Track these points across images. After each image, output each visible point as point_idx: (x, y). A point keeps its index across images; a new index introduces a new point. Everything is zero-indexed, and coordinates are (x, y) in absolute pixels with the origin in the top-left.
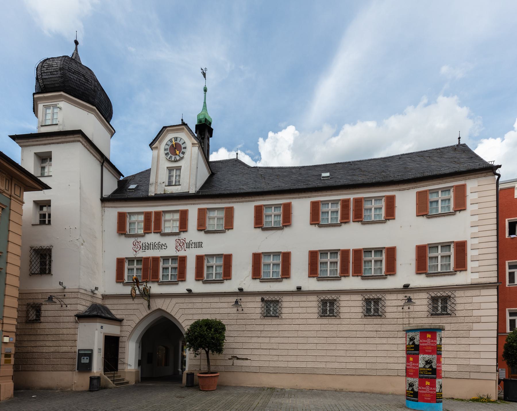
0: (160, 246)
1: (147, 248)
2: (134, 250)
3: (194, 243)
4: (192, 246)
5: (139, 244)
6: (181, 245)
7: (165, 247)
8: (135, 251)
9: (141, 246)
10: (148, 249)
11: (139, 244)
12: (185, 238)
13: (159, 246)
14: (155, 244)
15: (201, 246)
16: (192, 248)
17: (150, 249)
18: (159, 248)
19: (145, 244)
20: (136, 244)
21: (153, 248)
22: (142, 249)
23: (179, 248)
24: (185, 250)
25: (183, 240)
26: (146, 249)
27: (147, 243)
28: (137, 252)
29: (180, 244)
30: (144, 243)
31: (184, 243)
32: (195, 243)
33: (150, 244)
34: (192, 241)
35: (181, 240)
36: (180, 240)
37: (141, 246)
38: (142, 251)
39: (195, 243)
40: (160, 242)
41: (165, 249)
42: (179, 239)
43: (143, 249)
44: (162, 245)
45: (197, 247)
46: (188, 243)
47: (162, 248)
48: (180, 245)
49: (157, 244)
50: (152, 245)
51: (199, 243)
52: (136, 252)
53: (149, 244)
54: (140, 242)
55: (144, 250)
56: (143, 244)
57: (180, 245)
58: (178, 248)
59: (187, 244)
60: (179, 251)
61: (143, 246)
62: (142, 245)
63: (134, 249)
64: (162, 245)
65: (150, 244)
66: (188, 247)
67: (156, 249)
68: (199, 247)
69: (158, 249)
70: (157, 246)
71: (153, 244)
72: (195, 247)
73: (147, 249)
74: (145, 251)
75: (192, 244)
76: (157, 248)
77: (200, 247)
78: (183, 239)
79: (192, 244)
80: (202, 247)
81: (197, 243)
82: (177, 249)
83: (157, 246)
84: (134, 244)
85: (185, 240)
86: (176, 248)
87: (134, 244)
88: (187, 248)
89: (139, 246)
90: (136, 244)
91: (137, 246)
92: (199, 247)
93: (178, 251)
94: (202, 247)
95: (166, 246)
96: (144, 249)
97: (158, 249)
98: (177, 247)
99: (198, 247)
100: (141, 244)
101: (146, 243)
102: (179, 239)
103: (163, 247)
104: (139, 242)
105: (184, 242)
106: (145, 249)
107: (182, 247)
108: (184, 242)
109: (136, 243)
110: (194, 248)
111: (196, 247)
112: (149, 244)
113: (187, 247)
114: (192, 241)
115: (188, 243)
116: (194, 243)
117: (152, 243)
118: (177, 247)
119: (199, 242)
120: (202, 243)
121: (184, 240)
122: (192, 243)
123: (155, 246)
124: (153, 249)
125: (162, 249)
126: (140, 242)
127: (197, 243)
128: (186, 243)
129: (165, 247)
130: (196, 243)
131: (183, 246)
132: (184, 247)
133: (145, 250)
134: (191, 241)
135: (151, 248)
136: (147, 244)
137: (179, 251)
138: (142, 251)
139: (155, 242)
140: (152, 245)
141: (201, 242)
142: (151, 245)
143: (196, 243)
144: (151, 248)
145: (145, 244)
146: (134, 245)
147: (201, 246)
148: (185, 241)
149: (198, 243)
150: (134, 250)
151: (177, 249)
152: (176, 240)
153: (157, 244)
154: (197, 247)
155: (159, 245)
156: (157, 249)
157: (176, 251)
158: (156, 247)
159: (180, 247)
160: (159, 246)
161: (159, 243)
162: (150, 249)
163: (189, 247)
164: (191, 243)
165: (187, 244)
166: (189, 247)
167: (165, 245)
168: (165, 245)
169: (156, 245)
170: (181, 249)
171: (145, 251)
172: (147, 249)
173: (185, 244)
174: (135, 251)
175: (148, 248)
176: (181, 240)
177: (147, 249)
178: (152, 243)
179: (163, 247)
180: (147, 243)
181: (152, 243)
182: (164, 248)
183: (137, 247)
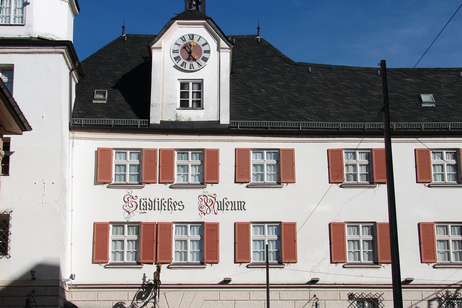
0: (172, 205)
1: (148, 207)
2: (125, 210)
3: (231, 202)
6: (209, 204)
7: (181, 208)
8: (128, 212)
9: (138, 204)
10: (150, 210)
12: (215, 194)
13: (171, 205)
14: (163, 201)
15: (242, 208)
16: (228, 210)
17: (155, 210)
20: (128, 201)
21: (160, 208)
22: (141, 209)
23: (205, 209)
24: (216, 214)
25: (211, 196)
26: (148, 208)
27: (149, 199)
29: (206, 204)
30: (144, 199)
31: (214, 201)
33: (155, 201)
34: (227, 199)
35: (209, 197)
36: (206, 196)
38: (140, 211)
40: (171, 199)
41: (181, 210)
42: (204, 196)
43: (142, 207)
44: (175, 204)
45: (236, 208)
46: (220, 202)
47: (175, 207)
48: (207, 205)
49: (166, 202)
50: (158, 202)
51: (239, 203)
52: (129, 213)
53: (153, 201)
54: (136, 196)
55: (143, 211)
56: (142, 200)
57: (207, 205)
58: (204, 209)
60: (205, 214)
61: (142, 203)
62: (140, 202)
64: (175, 204)
65: (155, 201)
66: (221, 209)
67: (165, 210)
68: (240, 208)
69: (169, 210)
71: (160, 201)
72: (233, 208)
75: (228, 204)
76: (166, 208)
77: (241, 210)
78: (213, 195)
79: (228, 204)
80: (245, 210)
81: (236, 203)
82: (201, 211)
84: (126, 200)
85: (214, 197)
87: (126, 200)
88: (219, 210)
90: (128, 201)
91: (130, 203)
92: (240, 208)
94: (245, 210)
95: (183, 205)
96: (144, 209)
97: (169, 210)
98: (201, 207)
100: (138, 201)
101: (146, 199)
102: (204, 196)
103: (177, 207)
104: (134, 197)
105: (213, 200)
106: (145, 208)
108: (213, 200)
110: (232, 210)
111: (235, 210)
112: (153, 201)
113: (219, 208)
114: (227, 199)
115: (220, 202)
116: (231, 202)
117: (158, 199)
118: (201, 207)
119: (240, 201)
120: (245, 203)
121: (213, 197)
122: (228, 202)
123: (163, 206)
124: (159, 209)
125: (175, 210)
127: (236, 203)
130: (234, 202)
132: (214, 208)
133: (145, 211)
134: (225, 199)
135: (156, 208)
136: (148, 201)
140: (158, 202)
141: (243, 202)
142: (156, 203)
143: (234, 202)
144: (156, 208)
145: (145, 200)
146: (126, 202)
147: (242, 208)
148: (215, 198)
149: (238, 202)
150: (125, 210)
151: (201, 211)
152: (200, 196)
153: (166, 202)
154: (236, 208)
155: (170, 204)
156: (167, 210)
157: (201, 214)
158: (165, 206)
159: (207, 207)
160: (171, 205)
161: (170, 200)
162: (155, 210)
163: (222, 208)
164: (225, 202)
166: (222, 208)
167: (180, 204)
168: (180, 203)
169: (165, 204)
172: (149, 209)
173: (216, 204)
174: (128, 212)
175: (150, 208)
176: (209, 197)
178: (156, 200)
179: (177, 207)
180: (149, 199)
181: (158, 199)
182: (179, 209)
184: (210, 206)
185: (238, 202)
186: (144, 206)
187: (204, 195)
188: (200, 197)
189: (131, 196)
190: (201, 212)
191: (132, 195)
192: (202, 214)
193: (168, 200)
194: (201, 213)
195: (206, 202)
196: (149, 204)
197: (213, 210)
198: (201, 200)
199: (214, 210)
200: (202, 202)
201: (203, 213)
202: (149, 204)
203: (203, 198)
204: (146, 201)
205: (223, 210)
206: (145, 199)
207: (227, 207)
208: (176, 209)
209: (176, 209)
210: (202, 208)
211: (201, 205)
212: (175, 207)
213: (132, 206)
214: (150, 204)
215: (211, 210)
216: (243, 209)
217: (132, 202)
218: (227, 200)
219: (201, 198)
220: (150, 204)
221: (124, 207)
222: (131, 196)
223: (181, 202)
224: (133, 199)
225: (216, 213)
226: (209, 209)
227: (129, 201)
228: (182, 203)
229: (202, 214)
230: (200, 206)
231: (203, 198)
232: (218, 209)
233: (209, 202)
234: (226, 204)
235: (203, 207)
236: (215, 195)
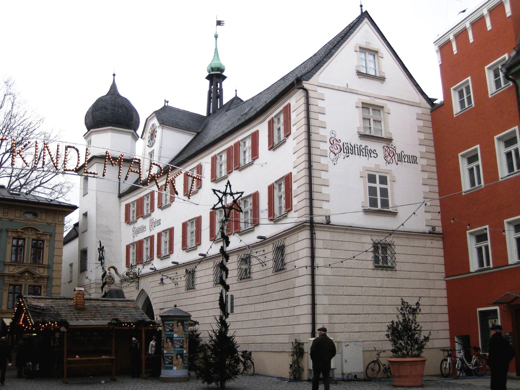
0: (368, 152)
1: (350, 151)
2: (332, 151)
3: (407, 155)
4: (405, 159)
5: (339, 144)
6: (391, 155)
7: (375, 155)
8: (334, 153)
9: (342, 147)
11: (339, 144)
14: (361, 148)
15: (415, 162)
16: (404, 161)
17: (355, 154)
18: (367, 155)
20: (334, 143)
21: (359, 154)
22: (344, 152)
23: (389, 158)
24: (397, 164)
25: (392, 148)
26: (350, 152)
28: (337, 155)
29: (389, 154)
30: (346, 143)
31: (395, 153)
33: (355, 147)
34: (403, 152)
35: (391, 149)
37: (342, 147)
40: (367, 147)
41: (375, 158)
42: (387, 147)
45: (411, 161)
46: (399, 154)
47: (371, 155)
48: (390, 156)
50: (357, 148)
51: (413, 157)
52: (335, 155)
53: (353, 146)
54: (339, 140)
56: (345, 144)
57: (390, 156)
62: (343, 145)
67: (363, 156)
68: (413, 162)
69: (366, 156)
70: (364, 151)
72: (409, 161)
73: (351, 153)
75: (405, 157)
76: (364, 154)
77: (415, 163)
80: (417, 164)
82: (386, 160)
83: (364, 151)
84: (332, 142)
85: (395, 149)
86: (386, 159)
87: (332, 142)
92: (413, 162)
93: (388, 163)
94: (417, 164)
95: (376, 154)
97: (366, 156)
98: (386, 157)
99: (413, 163)
100: (341, 144)
101: (348, 143)
103: (372, 155)
104: (338, 140)
105: (394, 151)
106: (347, 152)
108: (394, 151)
109: (334, 141)
111: (411, 163)
112: (353, 146)
113: (399, 160)
114: (403, 152)
117: (357, 145)
122: (404, 155)
128: (397, 154)
129: (375, 155)
132: (395, 159)
133: (348, 154)
135: (356, 153)
136: (350, 146)
137: (389, 163)
139: (361, 145)
140: (357, 148)
141: (415, 156)
144: (356, 153)
146: (331, 144)
147: (415, 162)
148: (395, 150)
152: (384, 147)
153: (363, 148)
154: (411, 161)
158: (363, 153)
159: (390, 158)
161: (366, 148)
163: (401, 160)
164: (403, 155)
166: (401, 160)
167: (374, 151)
168: (374, 151)
170: (391, 162)
173: (396, 155)
174: (334, 153)
175: (352, 152)
177: (350, 154)
178: (356, 146)
179: (372, 155)
181: (357, 145)
182: (374, 157)
183: (336, 148)
184: (392, 156)
185: (411, 156)
194: (386, 161)
197: (395, 161)
198: (385, 150)
203: (386, 149)
204: (348, 145)
207: (405, 159)
209: (371, 156)
214: (351, 148)
220: (351, 148)
222: (335, 139)
223: (375, 150)
224: (337, 143)
228: (376, 151)
231: (386, 149)
232: (398, 160)
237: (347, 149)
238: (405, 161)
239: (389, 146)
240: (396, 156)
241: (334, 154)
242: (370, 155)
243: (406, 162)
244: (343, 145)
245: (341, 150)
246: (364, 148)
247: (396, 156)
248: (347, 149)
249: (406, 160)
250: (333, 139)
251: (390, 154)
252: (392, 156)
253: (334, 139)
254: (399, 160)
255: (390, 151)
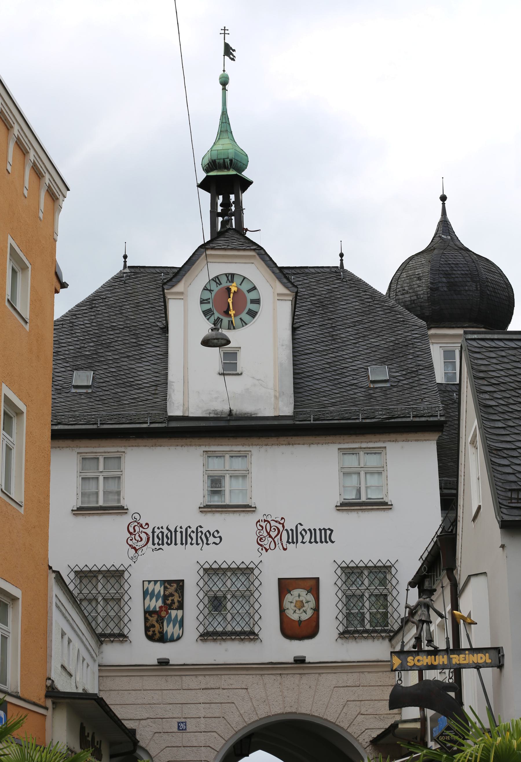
0: (203, 537)
1: (165, 540)
2: (130, 545)
3: (310, 530)
4: (303, 537)
5: (144, 530)
6: (273, 534)
8: (134, 548)
9: (151, 535)
11: (144, 530)
12: (282, 518)
13: (201, 537)
14: (189, 531)
15: (328, 540)
16: (303, 542)
17: (176, 544)
18: (199, 541)
19: (159, 531)
20: (135, 531)
21: (184, 542)
22: (154, 544)
23: (267, 542)
24: (285, 549)
25: (276, 521)
27: (167, 529)
29: (269, 533)
30: (158, 528)
31: (281, 529)
32: (313, 531)
33: (176, 531)
35: (273, 523)
36: (269, 522)
38: (154, 547)
39: (313, 531)
40: (201, 527)
42: (265, 521)
43: (156, 541)
44: (208, 534)
45: (318, 540)
46: (292, 530)
47: (207, 540)
48: (270, 536)
49: (193, 532)
50: (181, 532)
51: (323, 531)
52: (136, 550)
53: (173, 530)
54: (147, 524)
55: (157, 546)
56: (156, 530)
57: (270, 536)
58: (265, 542)
59: (290, 532)
60: (267, 550)
61: (156, 534)
62: (153, 532)
63: (130, 542)
64: (208, 534)
65: (176, 531)
66: (292, 541)
67: (191, 544)
68: (323, 540)
70: (194, 535)
71: (184, 530)
72: (313, 540)
74: (160, 549)
75: (303, 533)
76: (194, 541)
77: (327, 542)
78: (279, 519)
79: (303, 533)
80: (333, 542)
81: (318, 532)
82: (261, 545)
83: (194, 535)
84: (131, 530)
85: (282, 522)
87: (131, 530)
88: (289, 543)
89: (144, 536)
90: (135, 531)
91: (137, 535)
92: (323, 540)
94: (333, 542)
95: (220, 537)
96: (159, 544)
98: (261, 539)
99: (321, 542)
100: (149, 531)
101: (162, 528)
102: (265, 521)
103: (211, 540)
104: (143, 525)
106: (160, 542)
107: (276, 539)
109: (137, 528)
110: (310, 542)
111: (316, 542)
112: (173, 530)
113: (290, 540)
115: (292, 530)
116: (310, 530)
117: (181, 528)
118: (261, 539)
119: (324, 529)
120: (332, 531)
121: (280, 523)
122: (304, 530)
123: (189, 538)
124: (182, 544)
125: (207, 544)
126: (147, 526)
127: (318, 532)
128: (287, 530)
129: (217, 540)
130: (315, 530)
131: (279, 536)
132: (281, 540)
133: (161, 546)
136: (166, 532)
138: (154, 547)
140: (181, 532)
141: (329, 529)
142: (179, 535)
143: (315, 530)
145: (161, 530)
146: (131, 533)
147: (328, 540)
148: (283, 524)
149: (320, 530)
150: (130, 545)
151: (261, 545)
152: (259, 521)
153: (193, 532)
154: (318, 540)
155: (199, 534)
158: (192, 539)
159: (270, 539)
160: (201, 537)
161: (199, 529)
162: (176, 544)
163: (295, 541)
164: (300, 528)
165: (290, 532)
166: (295, 541)
167: (216, 534)
168: (216, 534)
169: (192, 534)
171: (160, 549)
172: (167, 543)
174: (134, 548)
175: (169, 542)
176: (273, 523)
178: (179, 529)
179: (211, 540)
180: (167, 529)
181: (181, 528)
182: (214, 543)
183: (137, 538)
184: (275, 537)
186: (159, 539)
187: (266, 519)
188: (259, 523)
189: (138, 523)
190: (260, 547)
191: (141, 522)
192: (262, 549)
193: (197, 529)
194: (261, 548)
195: (268, 530)
196: (167, 535)
199: (282, 544)
200: (262, 531)
201: (263, 548)
202: (167, 535)
203: (263, 524)
204: (162, 530)
205: (297, 542)
206: (160, 528)
207: (303, 537)
208: (209, 542)
209: (209, 542)
210: (262, 540)
211: (261, 537)
212: (207, 540)
213: (140, 540)
215: (277, 543)
216: (329, 542)
217: (140, 533)
218: (302, 528)
219: (260, 525)
221: (129, 540)
222: (138, 523)
225: (285, 547)
226: (273, 542)
227: (136, 532)
228: (218, 532)
229: (262, 549)
230: (259, 537)
231: (263, 524)
232: (288, 542)
233: (274, 530)
234: (301, 533)
235: (264, 539)
236: (283, 520)
237: (161, 538)
238: (304, 541)
239: (269, 519)
240: (285, 535)
241: (133, 550)
242: (205, 541)
243: (307, 543)
244: (153, 532)
245: (148, 539)
246: (195, 531)
247: (285, 535)
248: (161, 538)
249: (307, 538)
250: (133, 526)
251: (271, 533)
252: (275, 537)
253: (136, 524)
254: (290, 540)
255: (271, 527)
